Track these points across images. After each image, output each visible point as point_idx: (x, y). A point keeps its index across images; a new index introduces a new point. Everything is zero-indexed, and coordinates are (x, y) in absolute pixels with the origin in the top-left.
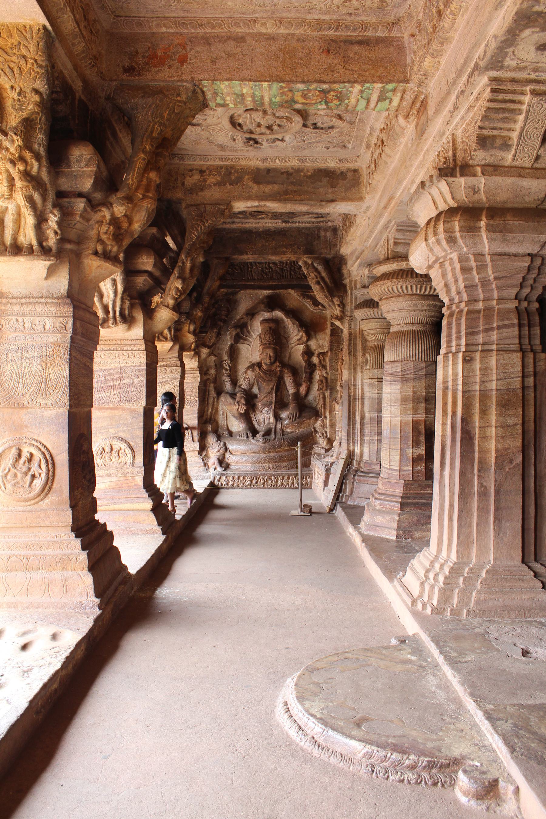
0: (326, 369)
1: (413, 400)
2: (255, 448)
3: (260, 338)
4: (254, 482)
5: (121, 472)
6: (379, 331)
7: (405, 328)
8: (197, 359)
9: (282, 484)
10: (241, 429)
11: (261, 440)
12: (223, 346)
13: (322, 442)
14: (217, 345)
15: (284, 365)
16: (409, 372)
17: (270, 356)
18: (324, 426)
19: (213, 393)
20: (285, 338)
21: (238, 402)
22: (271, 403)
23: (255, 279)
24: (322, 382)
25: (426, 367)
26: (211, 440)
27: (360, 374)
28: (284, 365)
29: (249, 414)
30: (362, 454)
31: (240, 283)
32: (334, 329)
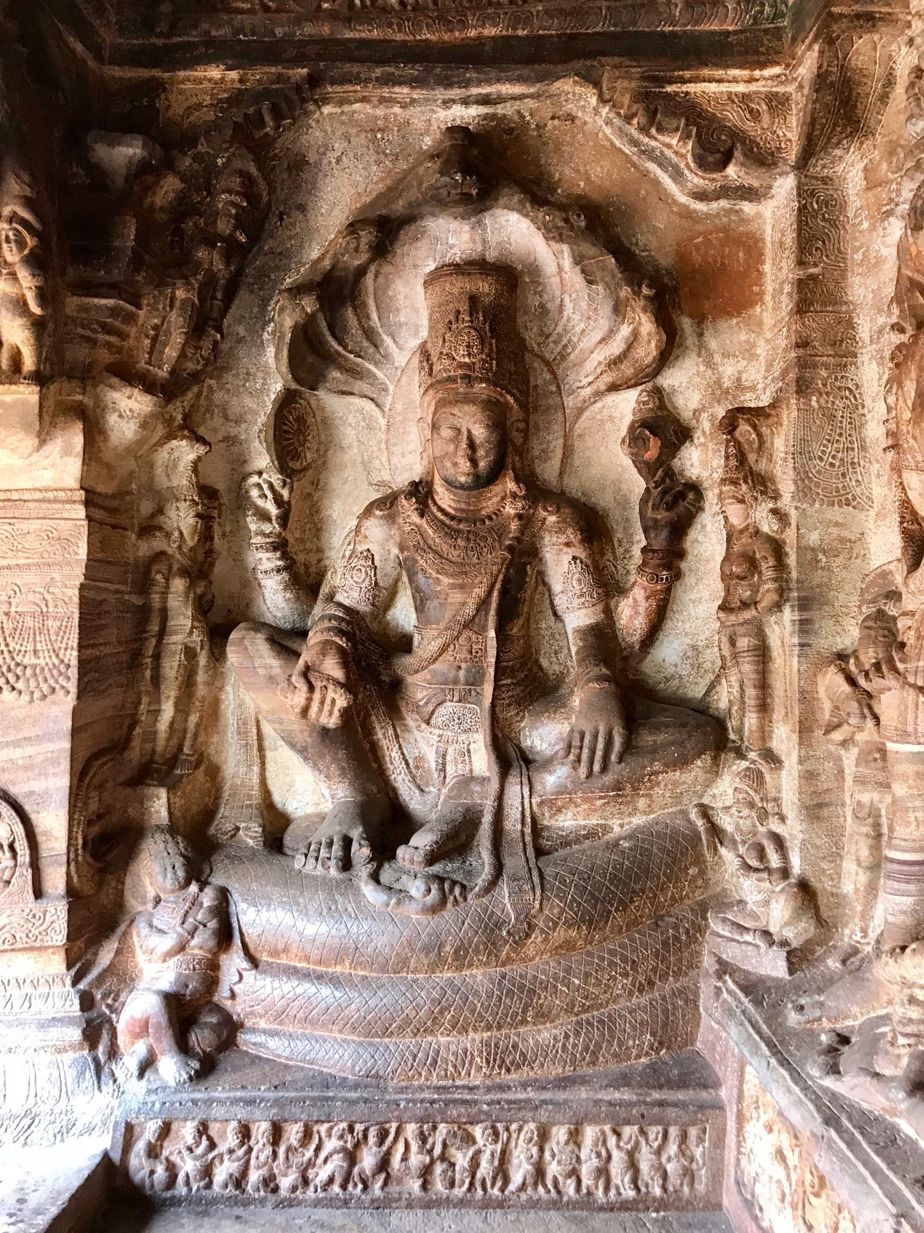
0: (776, 497)
4: (368, 1160)
8: (78, 440)
9: (540, 1172)
11: (416, 888)
12: (249, 402)
15: (537, 492)
17: (472, 445)
18: (764, 807)
19: (183, 626)
20: (547, 364)
21: (306, 674)
22: (475, 680)
26: (155, 872)
28: (537, 492)
29: (369, 732)
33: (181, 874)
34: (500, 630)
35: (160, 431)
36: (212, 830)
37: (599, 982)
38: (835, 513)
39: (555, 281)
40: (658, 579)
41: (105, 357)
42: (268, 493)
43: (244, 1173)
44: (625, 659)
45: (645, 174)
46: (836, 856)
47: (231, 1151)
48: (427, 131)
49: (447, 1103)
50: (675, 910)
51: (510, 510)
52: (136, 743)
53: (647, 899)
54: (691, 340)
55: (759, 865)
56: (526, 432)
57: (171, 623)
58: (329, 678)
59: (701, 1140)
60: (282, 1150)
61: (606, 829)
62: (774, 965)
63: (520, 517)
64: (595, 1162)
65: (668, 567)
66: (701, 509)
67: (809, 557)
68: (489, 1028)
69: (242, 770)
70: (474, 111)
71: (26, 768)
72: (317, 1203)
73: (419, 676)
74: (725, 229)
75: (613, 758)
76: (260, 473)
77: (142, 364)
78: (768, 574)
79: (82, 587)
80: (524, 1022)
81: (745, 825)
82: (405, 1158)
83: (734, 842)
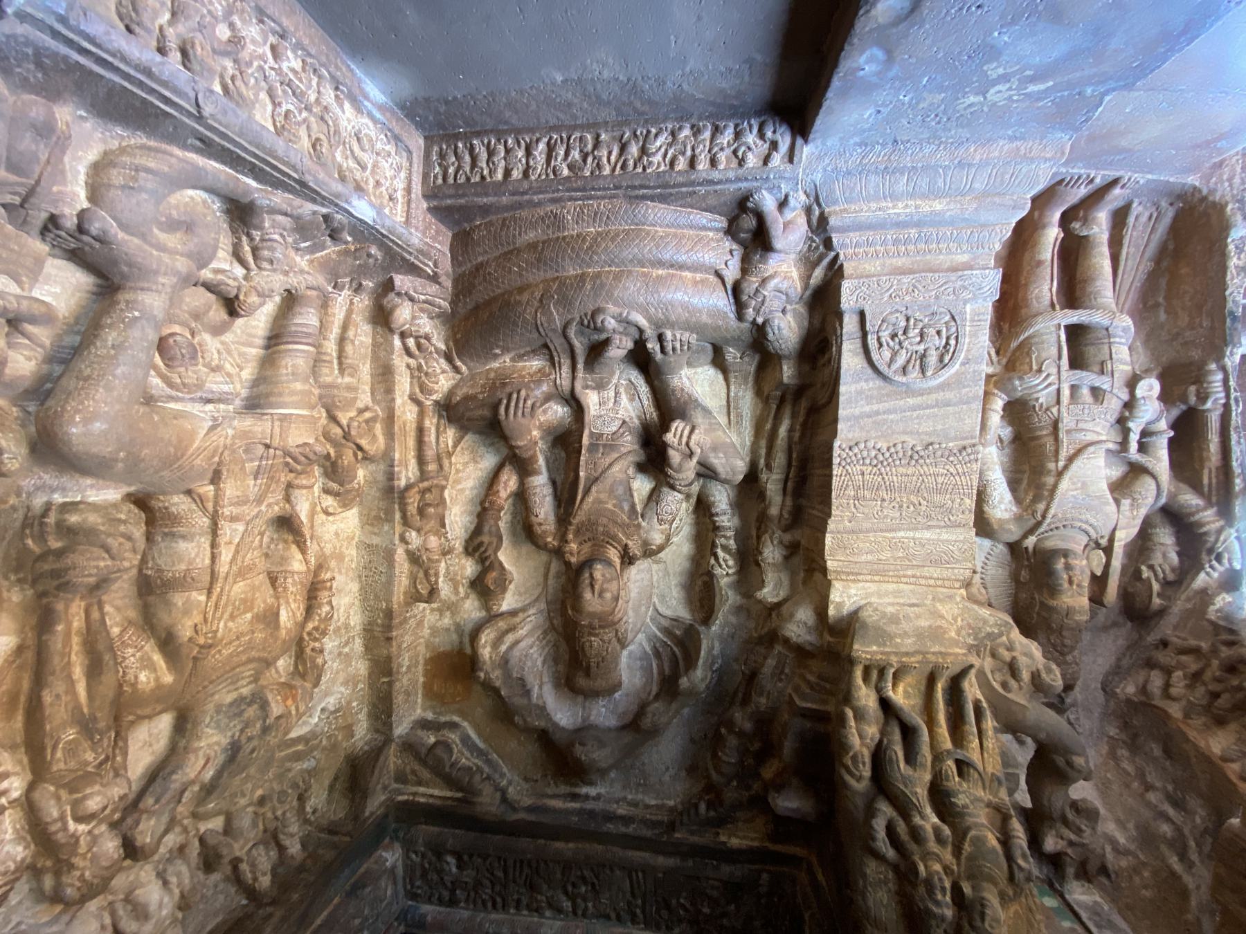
0: (408, 552)
4: (634, 150)
8: (831, 611)
10: (685, 372)
11: (611, 323)
17: (592, 586)
19: (772, 483)
21: (691, 455)
22: (593, 447)
26: (787, 329)
32: (384, 676)
33: (769, 330)
35: (784, 609)
36: (757, 357)
38: (376, 540)
39: (545, 679)
41: (815, 665)
45: (485, 741)
47: (722, 149)
48: (612, 780)
49: (584, 190)
51: (574, 546)
52: (802, 412)
53: (478, 319)
54: (466, 640)
55: (422, 341)
57: (780, 486)
58: (678, 450)
59: (436, 177)
60: (689, 153)
61: (513, 360)
62: (400, 280)
66: (467, 541)
68: (564, 238)
69: (740, 394)
70: (584, 790)
74: (443, 704)
77: (791, 656)
79: (829, 515)
80: (544, 242)
82: (610, 153)
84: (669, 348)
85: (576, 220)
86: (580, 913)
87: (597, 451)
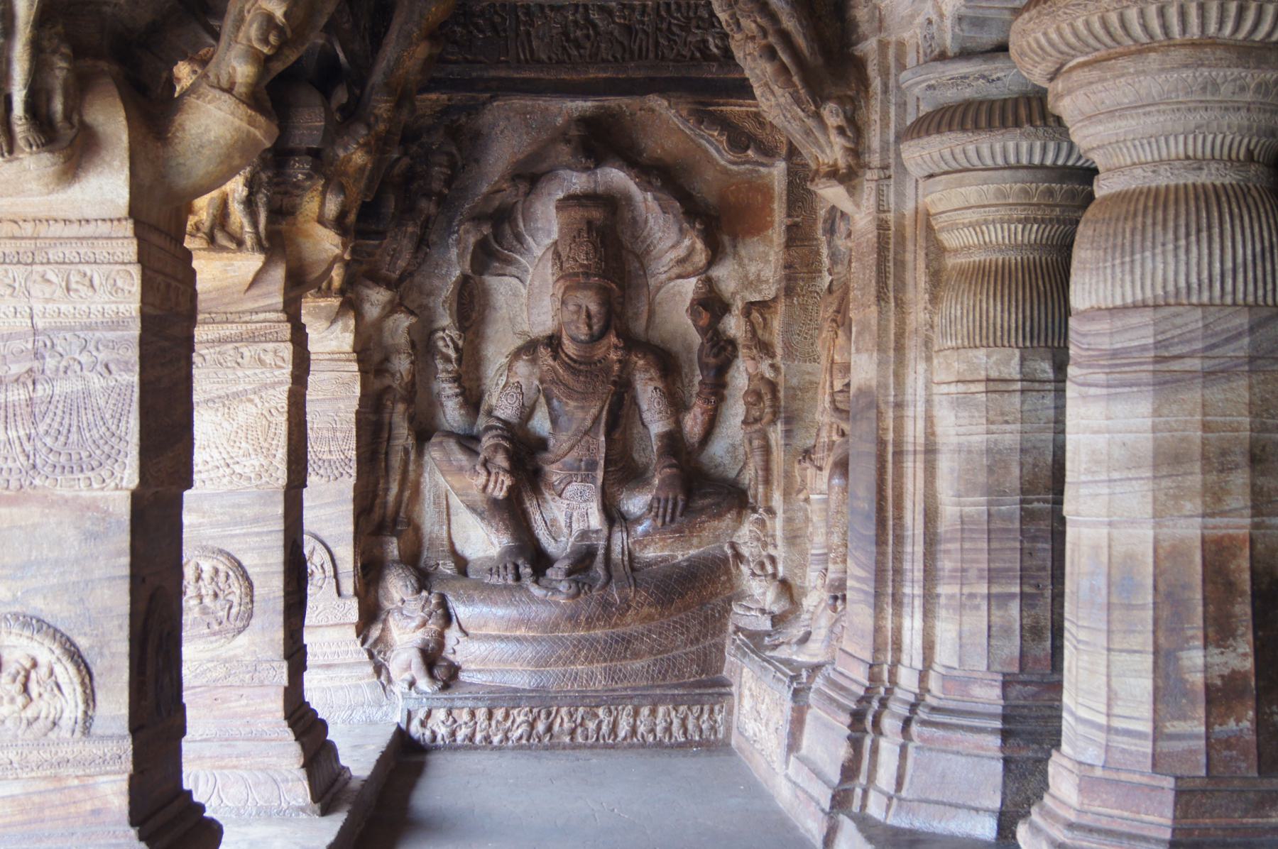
0: (773, 356)
1: (1205, 457)
2: (544, 613)
3: (557, 255)
4: (541, 727)
5: (34, 757)
6: (991, 214)
7: (1164, 179)
8: (352, 323)
9: (634, 731)
11: (563, 587)
12: (437, 282)
13: (762, 592)
14: (417, 279)
15: (632, 343)
16: (1185, 349)
17: (589, 316)
19: (403, 435)
22: (592, 466)
23: (539, 62)
24: (759, 396)
25: (1252, 330)
26: (397, 588)
27: (921, 367)
28: (632, 343)
29: (520, 502)
30: (928, 648)
31: (492, 73)
32: (796, 225)
34: (608, 435)
35: (388, 309)
36: (422, 564)
37: (667, 638)
38: (808, 366)
39: (642, 206)
40: (709, 402)
42: (451, 345)
43: (474, 734)
44: (689, 453)
45: (699, 146)
46: (803, 566)
50: (714, 601)
51: (613, 356)
53: (697, 593)
54: (729, 249)
56: (623, 304)
57: (395, 432)
58: (499, 467)
59: (720, 711)
60: (493, 723)
61: (674, 557)
63: (620, 361)
64: (664, 724)
65: (715, 394)
66: (736, 357)
67: (792, 392)
68: (605, 660)
69: (437, 528)
71: (326, 521)
72: (514, 748)
73: (554, 466)
75: (678, 513)
76: (444, 330)
77: (384, 271)
78: (768, 403)
79: (358, 413)
80: (625, 658)
81: (755, 551)
83: (748, 561)
84: (510, 567)
85: (592, 674)
86: (581, 9)
87: (587, 464)
